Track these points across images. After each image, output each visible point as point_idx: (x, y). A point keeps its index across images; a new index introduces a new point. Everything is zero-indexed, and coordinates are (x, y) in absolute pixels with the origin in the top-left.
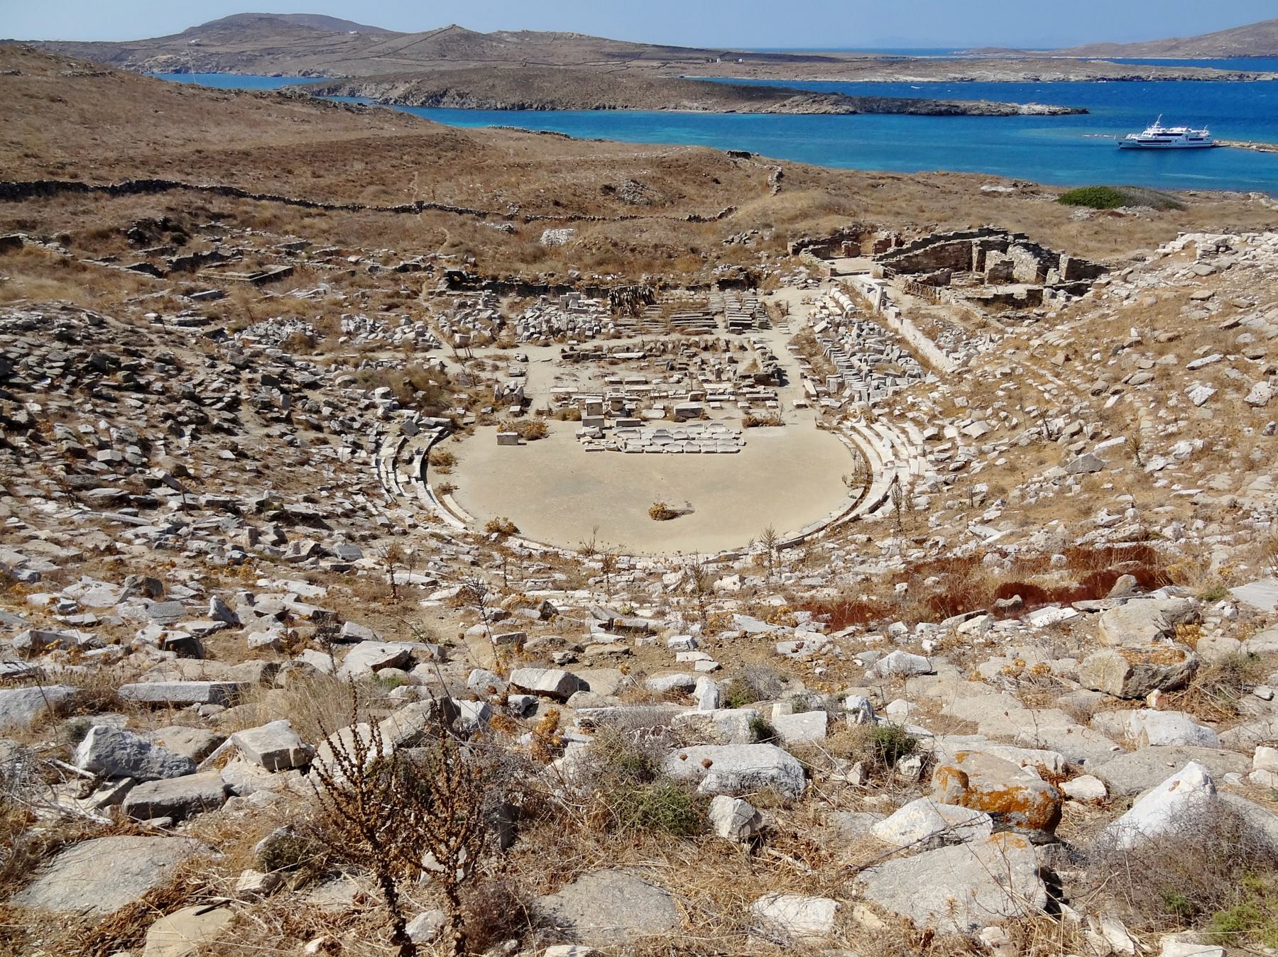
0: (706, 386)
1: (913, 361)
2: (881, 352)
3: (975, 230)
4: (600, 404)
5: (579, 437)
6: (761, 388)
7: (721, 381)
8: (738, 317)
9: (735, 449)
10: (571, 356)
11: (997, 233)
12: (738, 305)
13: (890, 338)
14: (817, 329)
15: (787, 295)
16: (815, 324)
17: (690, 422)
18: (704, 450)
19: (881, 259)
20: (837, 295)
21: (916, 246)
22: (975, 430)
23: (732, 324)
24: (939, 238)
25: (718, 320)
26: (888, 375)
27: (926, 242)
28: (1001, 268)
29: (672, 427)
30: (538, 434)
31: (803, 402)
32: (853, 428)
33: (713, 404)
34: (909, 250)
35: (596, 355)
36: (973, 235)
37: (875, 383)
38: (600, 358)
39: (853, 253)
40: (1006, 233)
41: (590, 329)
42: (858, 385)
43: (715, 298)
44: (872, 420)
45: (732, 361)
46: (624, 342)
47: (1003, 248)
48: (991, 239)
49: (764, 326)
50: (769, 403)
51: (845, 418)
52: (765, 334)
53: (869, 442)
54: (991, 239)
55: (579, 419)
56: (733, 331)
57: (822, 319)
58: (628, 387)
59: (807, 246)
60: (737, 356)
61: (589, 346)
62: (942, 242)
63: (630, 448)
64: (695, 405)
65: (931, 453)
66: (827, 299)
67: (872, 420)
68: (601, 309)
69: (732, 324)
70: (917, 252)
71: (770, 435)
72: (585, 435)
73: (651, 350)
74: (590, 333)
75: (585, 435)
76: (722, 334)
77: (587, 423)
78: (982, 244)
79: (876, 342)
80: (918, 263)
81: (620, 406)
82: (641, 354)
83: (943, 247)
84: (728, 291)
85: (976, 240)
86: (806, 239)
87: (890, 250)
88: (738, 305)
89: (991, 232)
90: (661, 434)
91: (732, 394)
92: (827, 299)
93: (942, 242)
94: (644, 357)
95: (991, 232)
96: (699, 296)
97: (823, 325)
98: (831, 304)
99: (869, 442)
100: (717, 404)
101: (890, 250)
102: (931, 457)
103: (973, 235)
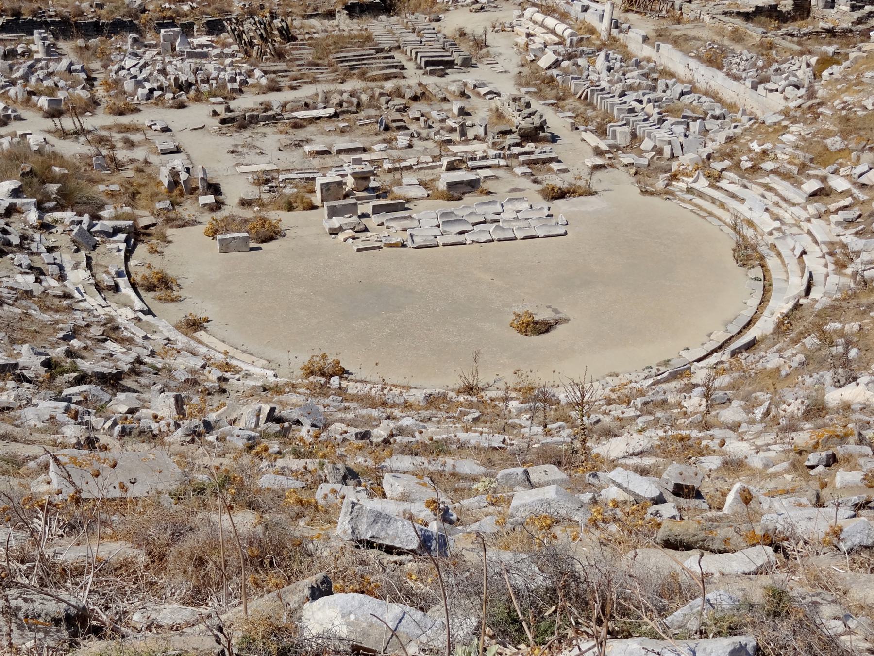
6: (529, 147)
7: (467, 142)
9: (562, 231)
10: (232, 120)
17: (468, 199)
18: (519, 235)
35: (267, 117)
38: (274, 119)
41: (232, 80)
44: (715, 179)
51: (674, 177)
56: (432, 73)
67: (715, 179)
73: (340, 104)
74: (236, 86)
94: (336, 115)
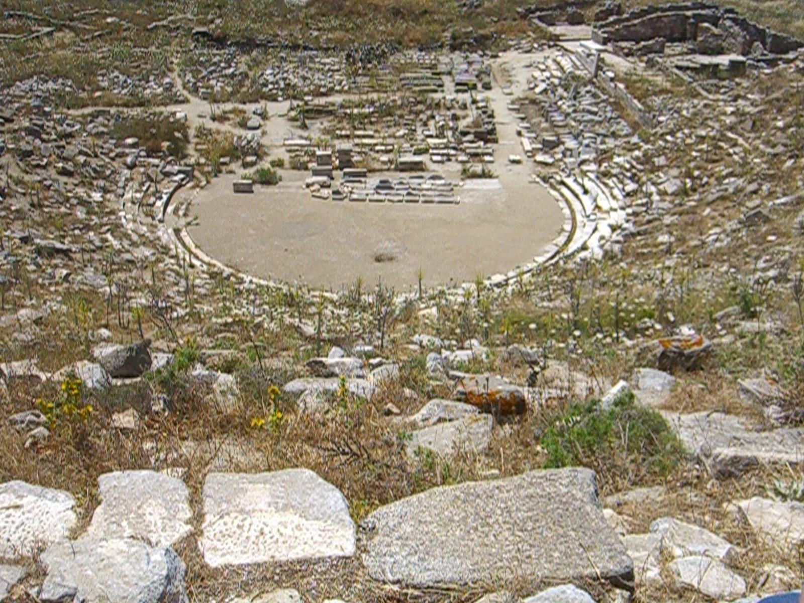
0: (430, 140)
1: (623, 123)
2: (595, 114)
3: (689, 4)
4: (329, 156)
5: (308, 186)
8: (464, 78)
11: (709, 7)
12: (465, 67)
13: (603, 101)
14: (537, 90)
15: (511, 58)
16: (536, 86)
18: (422, 199)
19: (602, 26)
20: (559, 59)
21: (634, 16)
22: (670, 187)
23: (458, 84)
24: (656, 10)
25: (446, 80)
26: (598, 135)
27: (644, 13)
28: (710, 40)
29: (394, 178)
30: (268, 179)
31: (517, 158)
32: (562, 183)
33: (435, 158)
34: (627, 20)
36: (687, 8)
37: (586, 142)
38: (330, 113)
39: (576, 20)
40: (717, 8)
41: (325, 86)
42: (571, 143)
43: (445, 59)
45: (455, 118)
46: (355, 98)
47: (715, 21)
48: (703, 12)
49: (487, 87)
50: (487, 158)
52: (488, 94)
53: (576, 196)
54: (703, 12)
55: (306, 169)
56: (457, 91)
57: (543, 81)
58: (357, 141)
59: (533, 12)
60: (460, 113)
61: (322, 101)
62: (659, 14)
63: (354, 196)
64: (417, 159)
65: (629, 206)
66: (549, 62)
68: (336, 67)
69: (458, 84)
70: (636, 22)
71: (485, 187)
72: (313, 184)
75: (313, 184)
76: (449, 93)
77: (316, 173)
78: (694, 16)
79: (590, 104)
80: (636, 32)
81: (347, 158)
82: (371, 110)
83: (659, 17)
84: (457, 52)
85: (689, 13)
86: (533, 7)
87: (611, 19)
88: (465, 67)
89: (703, 7)
90: (384, 185)
91: (454, 148)
92: (549, 62)
93: (659, 14)
95: (703, 7)
96: (428, 58)
97: (542, 86)
98: (553, 66)
99: (576, 196)
100: (438, 158)
101: (611, 19)
102: (629, 211)
103: (687, 8)
